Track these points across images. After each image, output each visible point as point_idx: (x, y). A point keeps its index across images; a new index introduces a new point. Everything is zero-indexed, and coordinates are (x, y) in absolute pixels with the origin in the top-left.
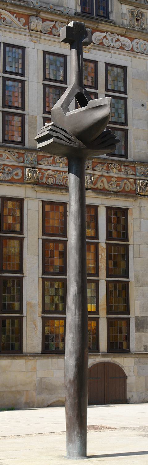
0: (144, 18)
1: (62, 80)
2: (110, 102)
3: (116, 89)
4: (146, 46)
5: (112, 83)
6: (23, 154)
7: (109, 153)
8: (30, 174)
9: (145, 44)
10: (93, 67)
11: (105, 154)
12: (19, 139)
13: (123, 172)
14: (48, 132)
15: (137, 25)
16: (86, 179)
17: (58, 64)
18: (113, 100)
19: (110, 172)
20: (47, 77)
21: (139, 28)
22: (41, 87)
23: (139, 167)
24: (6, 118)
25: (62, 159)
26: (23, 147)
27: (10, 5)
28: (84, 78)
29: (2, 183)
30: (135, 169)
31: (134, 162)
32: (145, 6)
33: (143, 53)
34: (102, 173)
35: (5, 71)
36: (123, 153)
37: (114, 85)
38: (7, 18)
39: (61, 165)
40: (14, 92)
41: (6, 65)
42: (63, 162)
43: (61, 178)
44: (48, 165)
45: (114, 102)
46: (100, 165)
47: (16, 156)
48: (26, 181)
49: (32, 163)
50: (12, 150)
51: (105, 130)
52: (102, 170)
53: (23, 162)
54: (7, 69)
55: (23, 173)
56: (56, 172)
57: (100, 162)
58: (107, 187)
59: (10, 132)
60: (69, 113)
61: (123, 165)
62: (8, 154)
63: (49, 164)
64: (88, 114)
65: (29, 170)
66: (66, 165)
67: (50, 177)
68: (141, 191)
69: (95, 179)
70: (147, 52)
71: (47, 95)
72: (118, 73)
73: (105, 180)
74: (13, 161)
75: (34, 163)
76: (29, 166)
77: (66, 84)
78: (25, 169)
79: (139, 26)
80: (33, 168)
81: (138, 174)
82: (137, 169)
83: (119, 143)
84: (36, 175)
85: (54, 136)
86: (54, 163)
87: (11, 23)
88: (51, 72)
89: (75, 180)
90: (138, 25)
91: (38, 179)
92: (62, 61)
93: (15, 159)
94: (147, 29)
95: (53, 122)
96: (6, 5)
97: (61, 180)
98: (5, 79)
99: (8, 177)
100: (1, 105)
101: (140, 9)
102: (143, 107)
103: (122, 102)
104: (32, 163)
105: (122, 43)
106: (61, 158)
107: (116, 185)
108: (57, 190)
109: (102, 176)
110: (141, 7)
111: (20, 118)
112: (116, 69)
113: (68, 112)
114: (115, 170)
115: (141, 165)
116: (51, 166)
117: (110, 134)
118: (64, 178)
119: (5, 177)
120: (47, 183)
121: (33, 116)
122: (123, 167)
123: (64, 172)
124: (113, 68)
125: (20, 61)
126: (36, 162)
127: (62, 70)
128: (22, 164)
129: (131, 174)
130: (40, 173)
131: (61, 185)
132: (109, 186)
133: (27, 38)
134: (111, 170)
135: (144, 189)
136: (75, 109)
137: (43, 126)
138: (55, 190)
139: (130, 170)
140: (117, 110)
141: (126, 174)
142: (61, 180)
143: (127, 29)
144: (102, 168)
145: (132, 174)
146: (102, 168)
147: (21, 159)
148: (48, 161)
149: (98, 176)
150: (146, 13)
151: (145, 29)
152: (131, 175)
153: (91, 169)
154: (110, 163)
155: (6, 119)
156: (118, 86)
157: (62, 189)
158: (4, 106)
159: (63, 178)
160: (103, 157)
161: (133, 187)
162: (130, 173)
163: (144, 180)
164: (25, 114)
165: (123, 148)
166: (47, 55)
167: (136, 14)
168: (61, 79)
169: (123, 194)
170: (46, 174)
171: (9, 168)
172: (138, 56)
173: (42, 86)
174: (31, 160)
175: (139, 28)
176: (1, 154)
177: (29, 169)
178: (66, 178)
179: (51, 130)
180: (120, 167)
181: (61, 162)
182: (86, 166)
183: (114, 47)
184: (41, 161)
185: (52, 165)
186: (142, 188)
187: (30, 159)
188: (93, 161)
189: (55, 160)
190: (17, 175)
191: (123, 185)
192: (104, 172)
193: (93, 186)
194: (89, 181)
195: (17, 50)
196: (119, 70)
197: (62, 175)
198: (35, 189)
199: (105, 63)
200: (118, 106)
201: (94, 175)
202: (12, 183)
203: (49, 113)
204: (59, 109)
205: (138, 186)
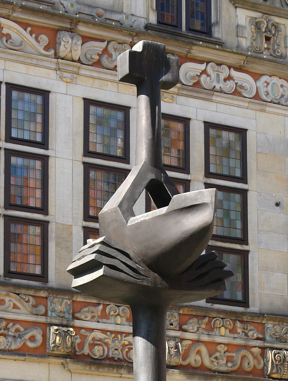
0: (282, 34)
1: (121, 155)
2: (214, 199)
3: (226, 173)
4: (285, 88)
5: (218, 162)
6: (45, 299)
7: (212, 296)
8: (58, 338)
9: (282, 86)
10: (181, 130)
11: (205, 300)
12: (38, 270)
13: (239, 333)
14: (93, 257)
15: (265, 48)
16: (167, 347)
17: (113, 124)
18: (220, 194)
19: (214, 333)
20: (91, 149)
21: (271, 55)
22: (80, 169)
23: (270, 325)
24: (12, 230)
25: (121, 308)
26: (44, 286)
27: (20, 10)
28: (163, 151)
29: (3, 354)
30: (262, 329)
31: (261, 315)
32: (282, 12)
33: (278, 104)
34: (199, 336)
35: (9, 139)
36: (239, 297)
37: (221, 165)
38: (14, 36)
39: (119, 320)
40: (27, 179)
41: (12, 126)
42: (122, 315)
43: (118, 344)
44: (92, 320)
45: (222, 199)
46: (195, 320)
47: (31, 303)
48: (50, 352)
49: (62, 317)
50: (23, 291)
51: (204, 253)
52: (198, 330)
53: (46, 314)
54: (14, 134)
55: (45, 337)
56: (109, 333)
57: (194, 314)
58: (207, 363)
59: (20, 256)
60: (134, 220)
61: (239, 321)
62: (16, 300)
63: (95, 319)
64: (172, 221)
65: (57, 330)
66: (127, 320)
67: (97, 345)
68: (274, 371)
69: (184, 348)
70: (286, 101)
71: (90, 184)
72: (238, 24)
73: (203, 349)
74: (26, 312)
75: (66, 317)
76: (57, 322)
77: (129, 163)
78: (48, 328)
79: (271, 51)
80: (63, 326)
81: (268, 338)
82: (266, 328)
83: (231, 278)
84: (70, 339)
85: (106, 265)
86: (104, 316)
87: (21, 45)
88: (99, 139)
89: (146, 349)
90: (268, 49)
91: (75, 348)
92: (121, 119)
93: (29, 309)
94: (286, 56)
95: (104, 237)
96: (11, 10)
97: (119, 350)
98: (9, 153)
99: (15, 343)
100: (2, 204)
101: (272, 17)
102: (278, 208)
103: (237, 197)
104: (62, 317)
105: (236, 84)
106: (118, 306)
107: (225, 359)
108: (111, 369)
109: (198, 341)
110: (274, 14)
111: (38, 230)
112: (225, 134)
113: (132, 219)
114: (223, 329)
115: (274, 321)
116: (98, 322)
117: (213, 259)
118: (124, 346)
119: (9, 344)
120: (91, 354)
121: (63, 224)
122: (238, 324)
123: (124, 335)
124: (219, 132)
125: (39, 118)
126: (69, 314)
127: (120, 135)
128: (42, 319)
129: (255, 338)
130: (78, 336)
131: (119, 359)
132: (213, 361)
133: (53, 74)
134: (215, 329)
135: (279, 366)
136: (146, 212)
137: (84, 245)
138: (106, 369)
139: (253, 330)
140: (227, 213)
141: (245, 337)
142: (119, 350)
143: (247, 56)
144: (198, 326)
145: (258, 339)
146: (198, 326)
147: (40, 309)
148: (92, 312)
149: (190, 342)
150: (284, 25)
151: (281, 57)
152: (254, 339)
153: (178, 329)
154: (214, 316)
155: (11, 231)
156: (229, 166)
157: (121, 367)
158: (8, 205)
159: (122, 346)
160: (200, 305)
161: (259, 363)
162: (253, 336)
163: (281, 349)
164: (49, 221)
165: (240, 288)
166: (91, 106)
167: (265, 26)
168: (119, 153)
169: (239, 376)
170: (90, 338)
171: (18, 326)
172: (268, 109)
173: (81, 167)
174: (61, 311)
175: (271, 55)
176: (1, 298)
177: (56, 328)
178: (127, 345)
179: (98, 252)
180: (234, 324)
181: (118, 315)
182: (168, 323)
183: (221, 91)
184: (79, 312)
185: (100, 320)
186: (277, 365)
187: (59, 308)
188: (181, 312)
189: (107, 311)
190: (32, 339)
191: (240, 359)
192: (203, 334)
193: (181, 362)
194: (173, 351)
195: (33, 97)
196: (232, 136)
197: (121, 340)
198: (69, 368)
199: (205, 123)
200: (230, 207)
201: (182, 340)
202: (24, 355)
203: (95, 219)
204: (114, 211)
205: (269, 361)
